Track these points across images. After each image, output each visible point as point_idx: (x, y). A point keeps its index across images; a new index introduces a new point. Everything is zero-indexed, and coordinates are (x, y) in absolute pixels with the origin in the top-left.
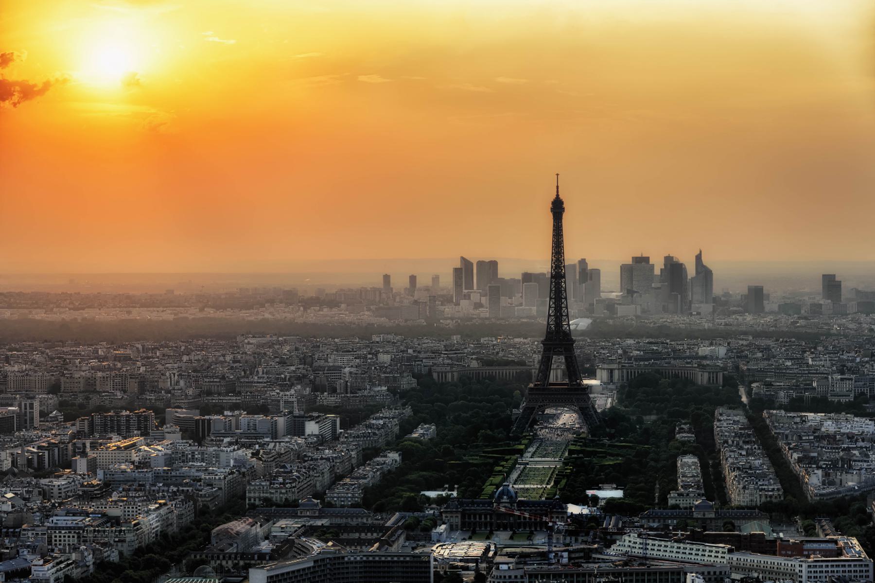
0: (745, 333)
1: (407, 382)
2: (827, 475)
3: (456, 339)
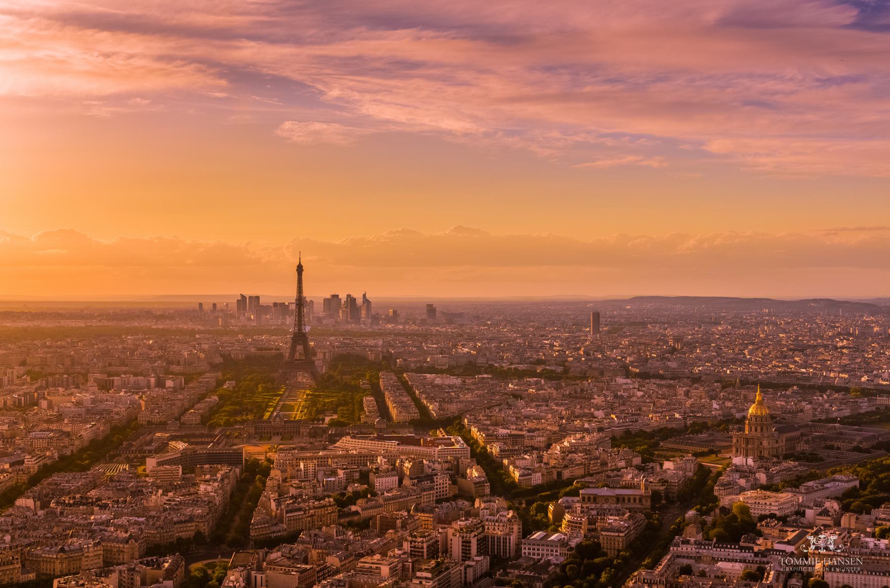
0: (390, 334)
1: (218, 360)
2: (440, 405)
3: (240, 337)
